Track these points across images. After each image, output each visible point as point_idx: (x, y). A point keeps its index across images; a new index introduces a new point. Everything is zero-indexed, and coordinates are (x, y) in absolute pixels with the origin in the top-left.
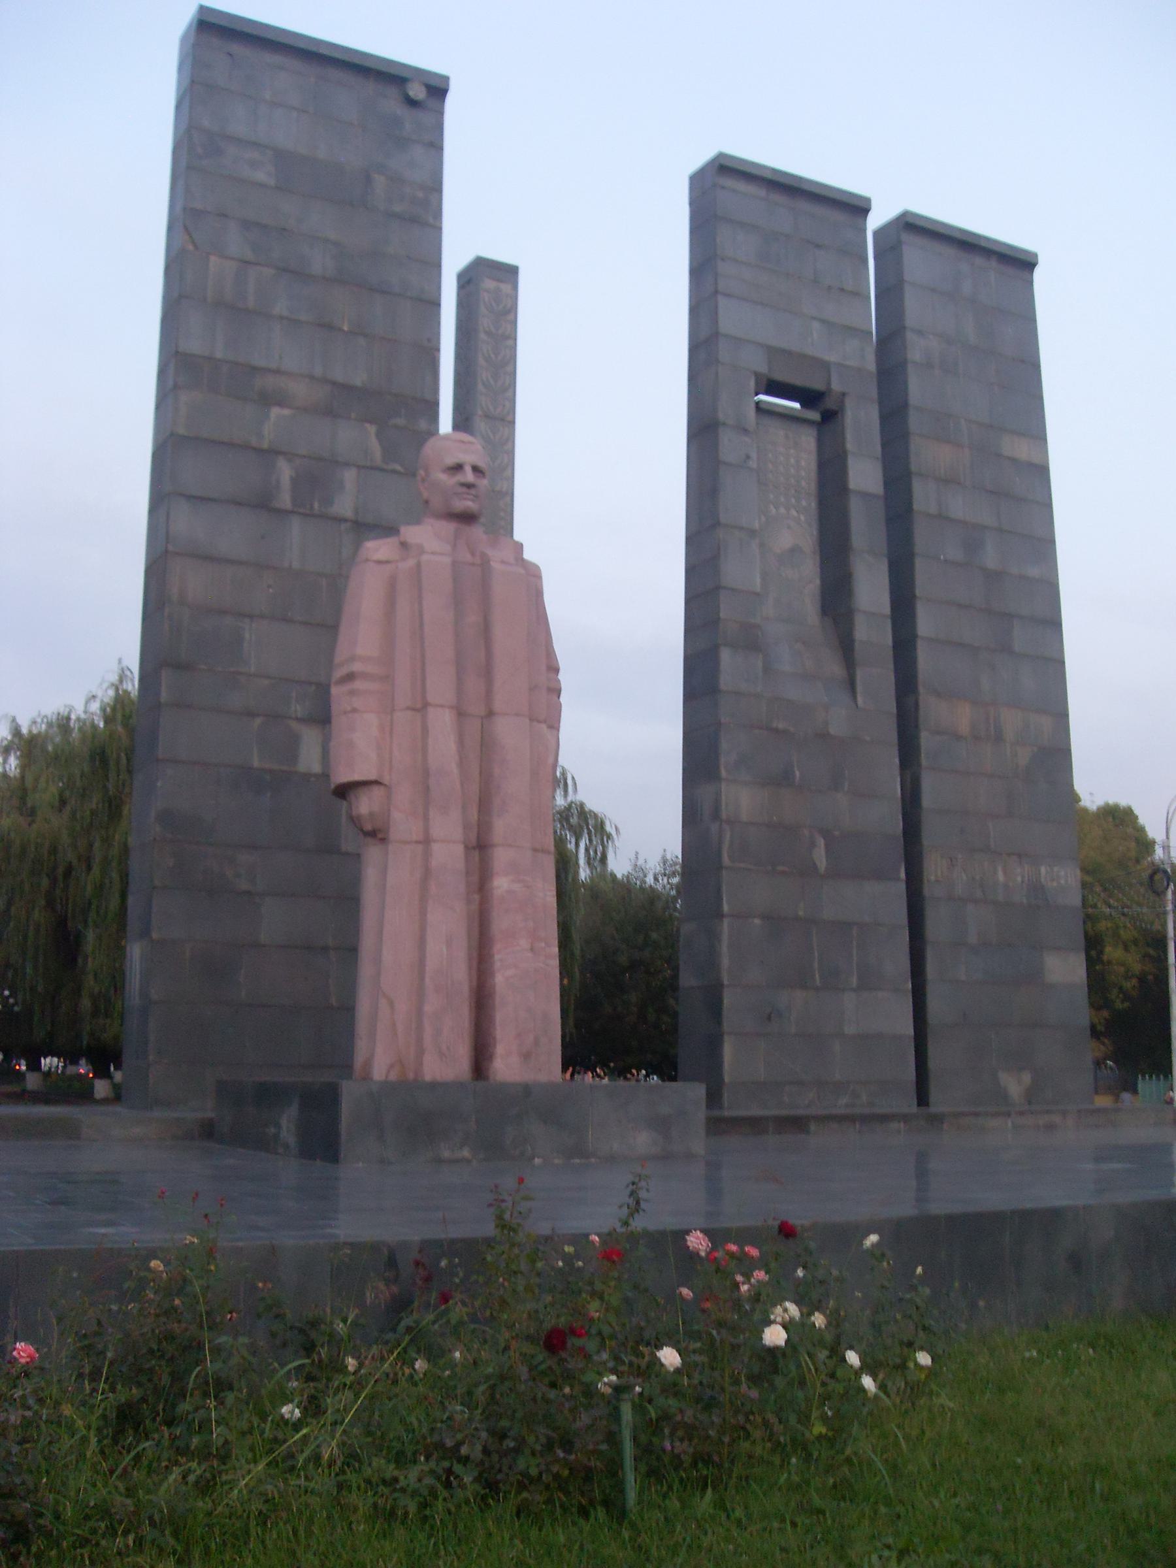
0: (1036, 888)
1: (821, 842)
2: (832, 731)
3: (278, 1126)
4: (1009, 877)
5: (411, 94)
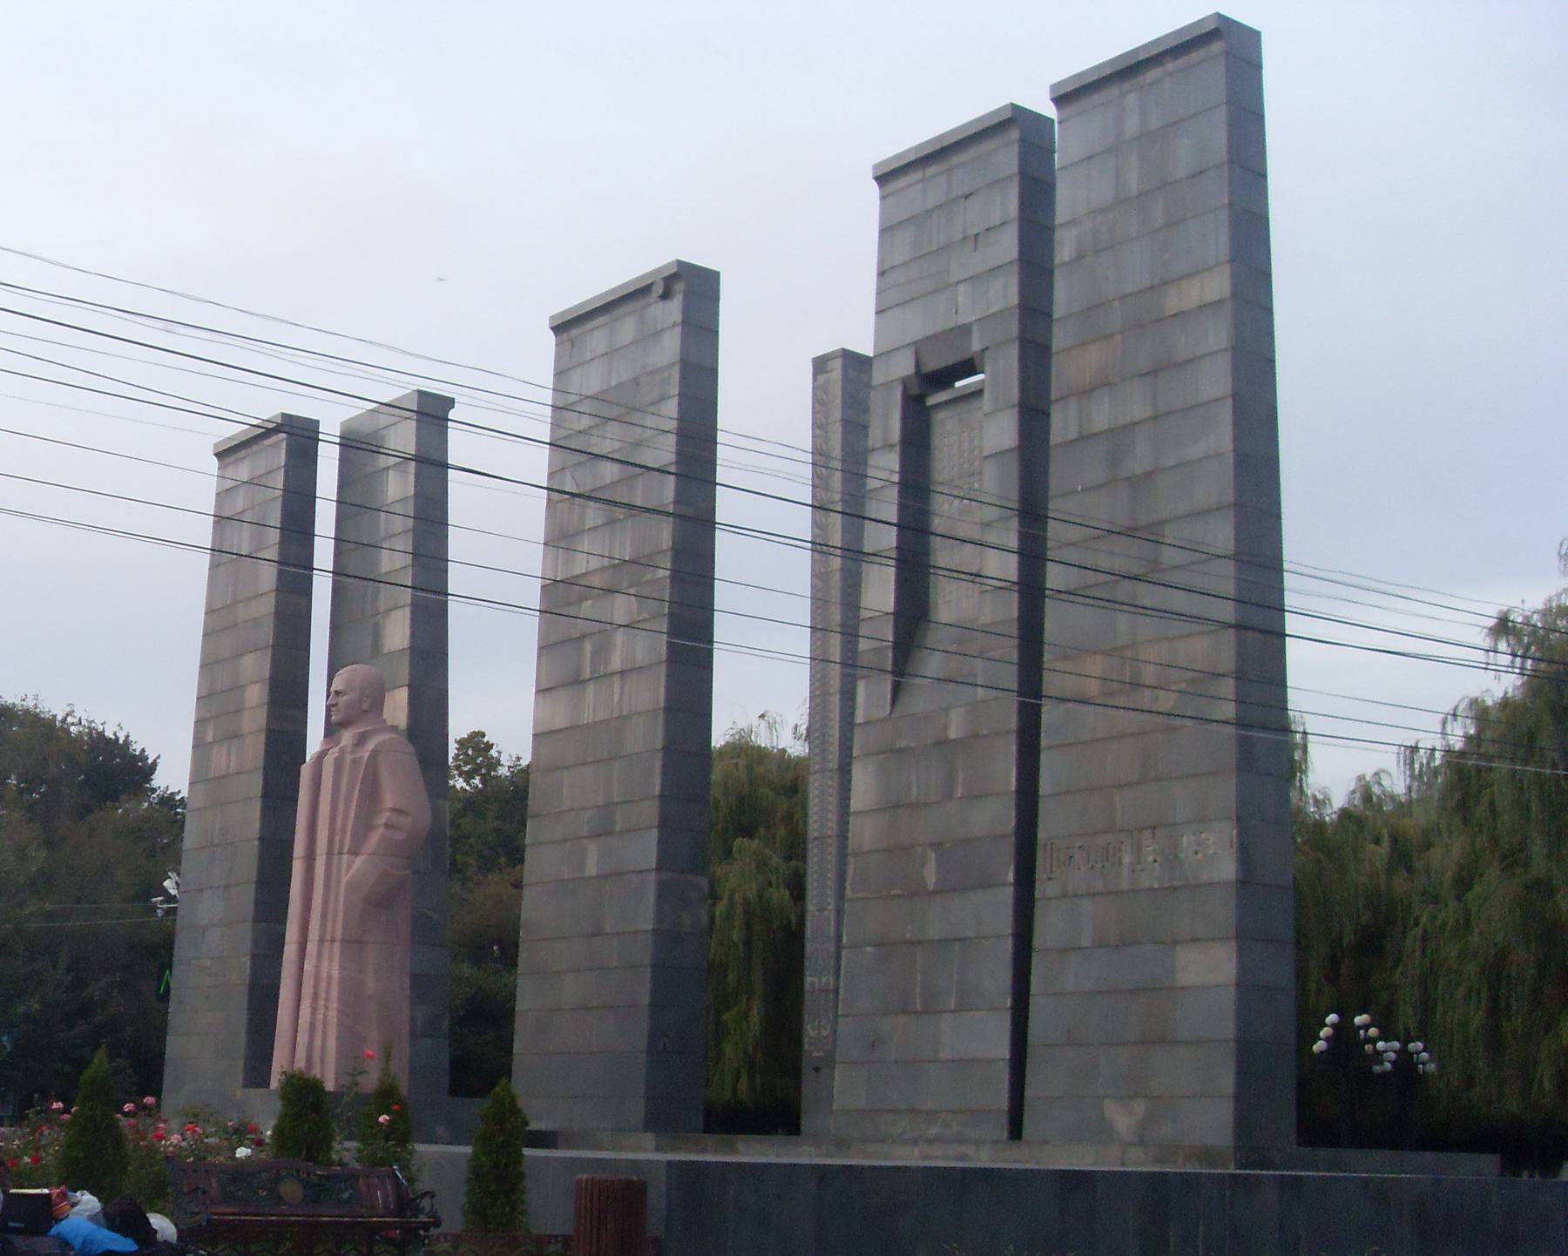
1: (932, 856)
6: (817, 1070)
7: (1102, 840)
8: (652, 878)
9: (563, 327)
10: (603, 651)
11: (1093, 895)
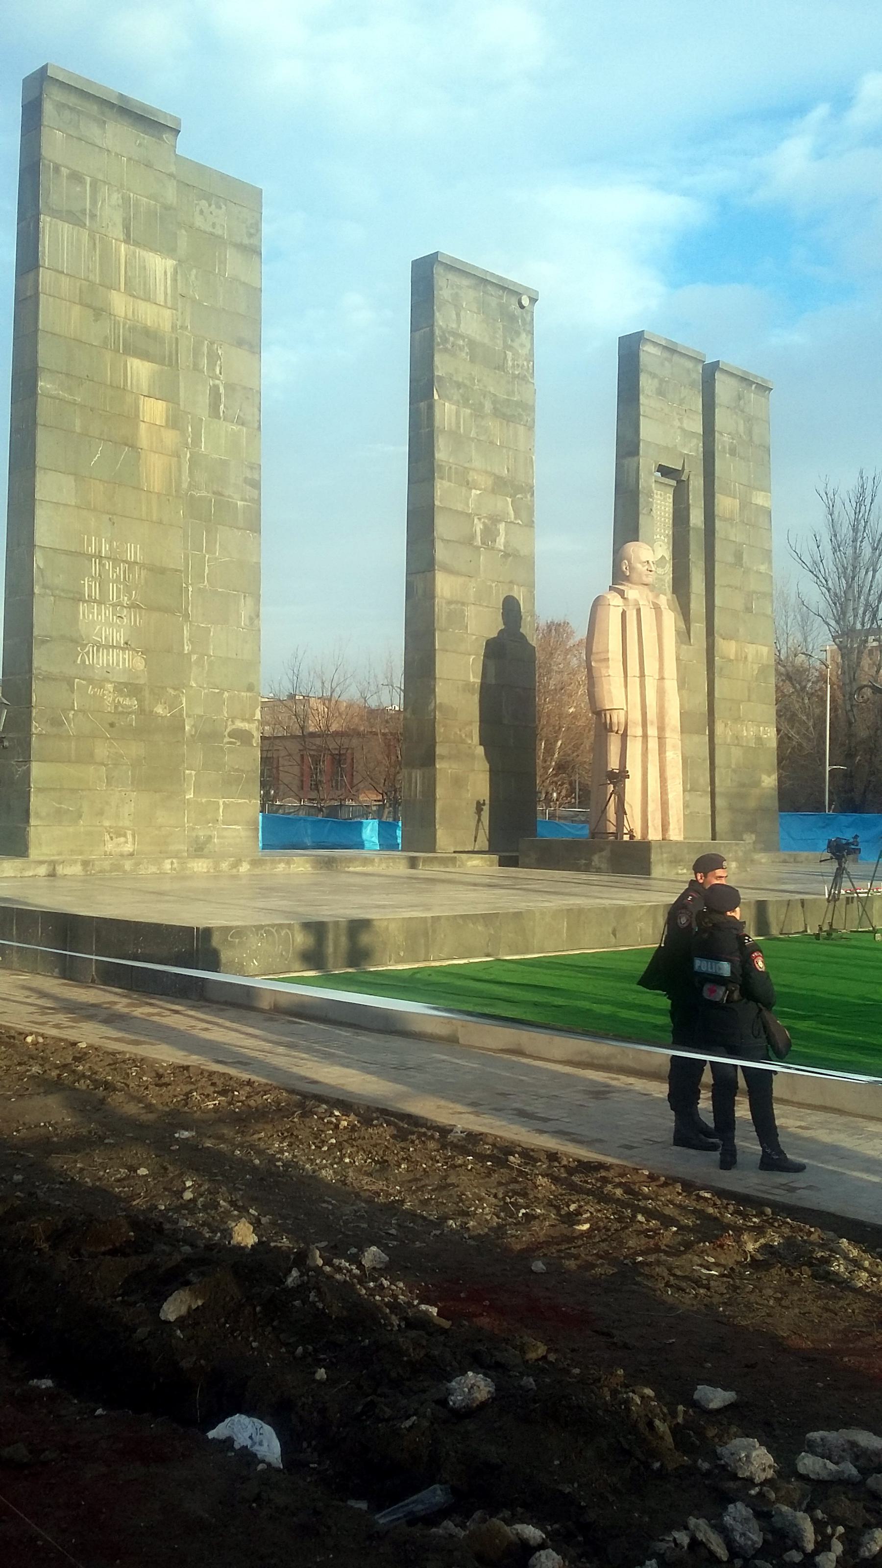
0: (759, 739)
3: (591, 861)
4: (748, 732)
5: (523, 302)
10: (490, 534)
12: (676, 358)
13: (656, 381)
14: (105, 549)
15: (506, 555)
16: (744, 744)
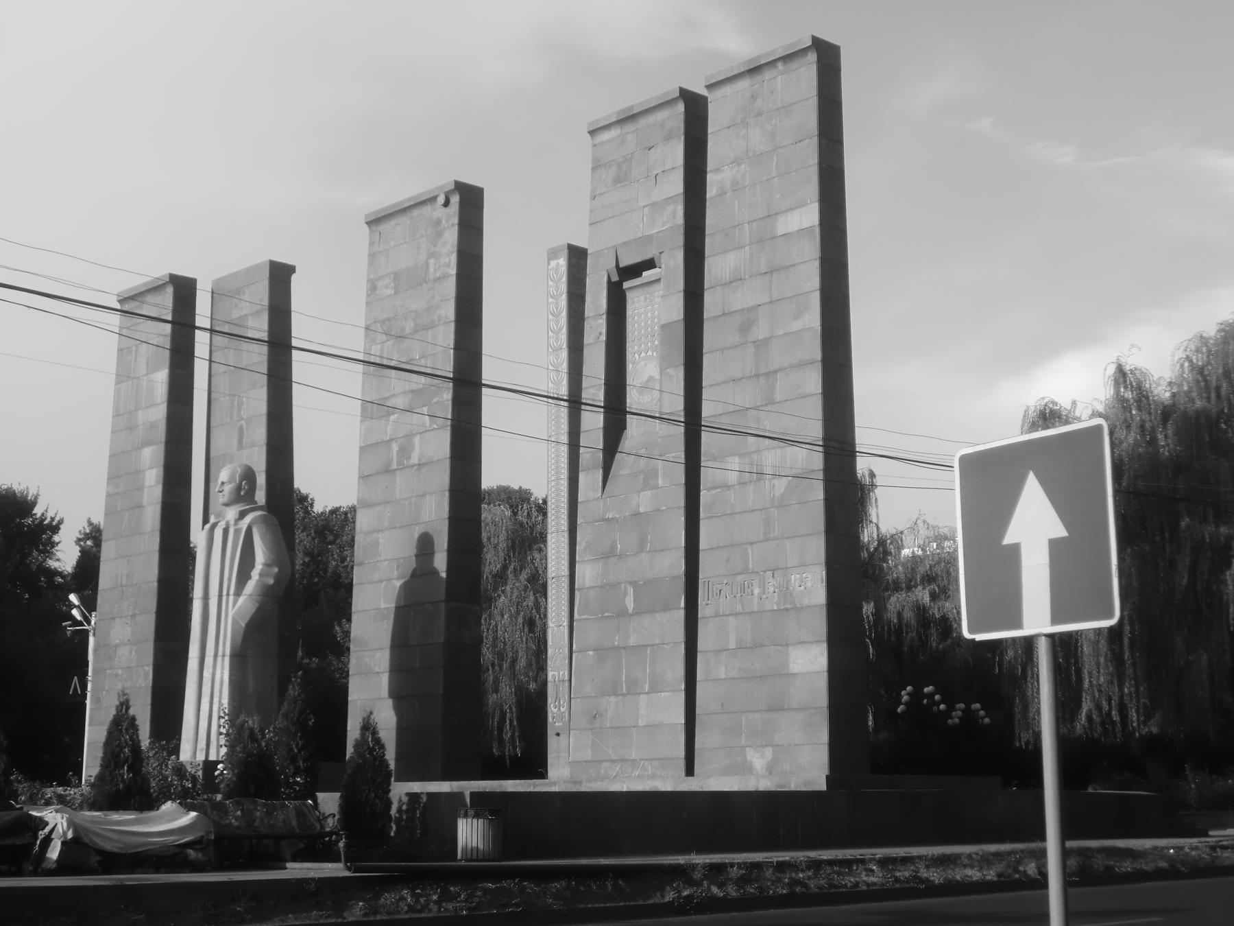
1: (631, 590)
2: (642, 510)
6: (558, 735)
7: (740, 578)
8: (442, 606)
9: (374, 222)
10: (405, 451)
11: (736, 614)
12: (642, 122)
13: (613, 171)
14: (124, 582)
15: (420, 465)
16: (756, 609)
